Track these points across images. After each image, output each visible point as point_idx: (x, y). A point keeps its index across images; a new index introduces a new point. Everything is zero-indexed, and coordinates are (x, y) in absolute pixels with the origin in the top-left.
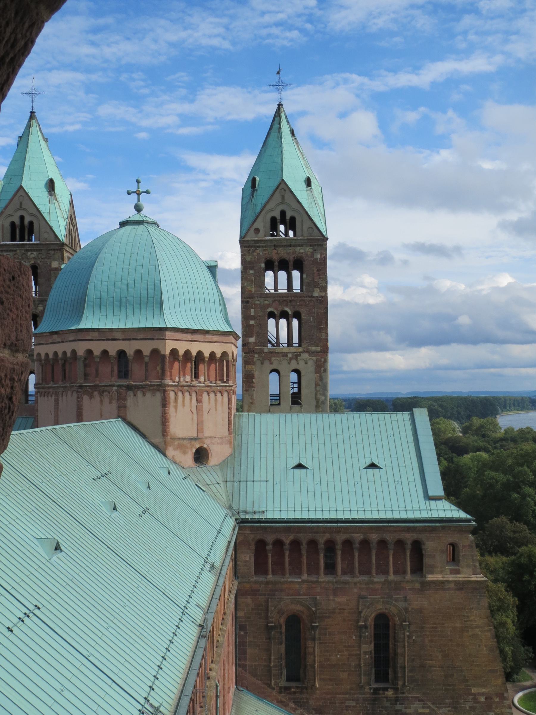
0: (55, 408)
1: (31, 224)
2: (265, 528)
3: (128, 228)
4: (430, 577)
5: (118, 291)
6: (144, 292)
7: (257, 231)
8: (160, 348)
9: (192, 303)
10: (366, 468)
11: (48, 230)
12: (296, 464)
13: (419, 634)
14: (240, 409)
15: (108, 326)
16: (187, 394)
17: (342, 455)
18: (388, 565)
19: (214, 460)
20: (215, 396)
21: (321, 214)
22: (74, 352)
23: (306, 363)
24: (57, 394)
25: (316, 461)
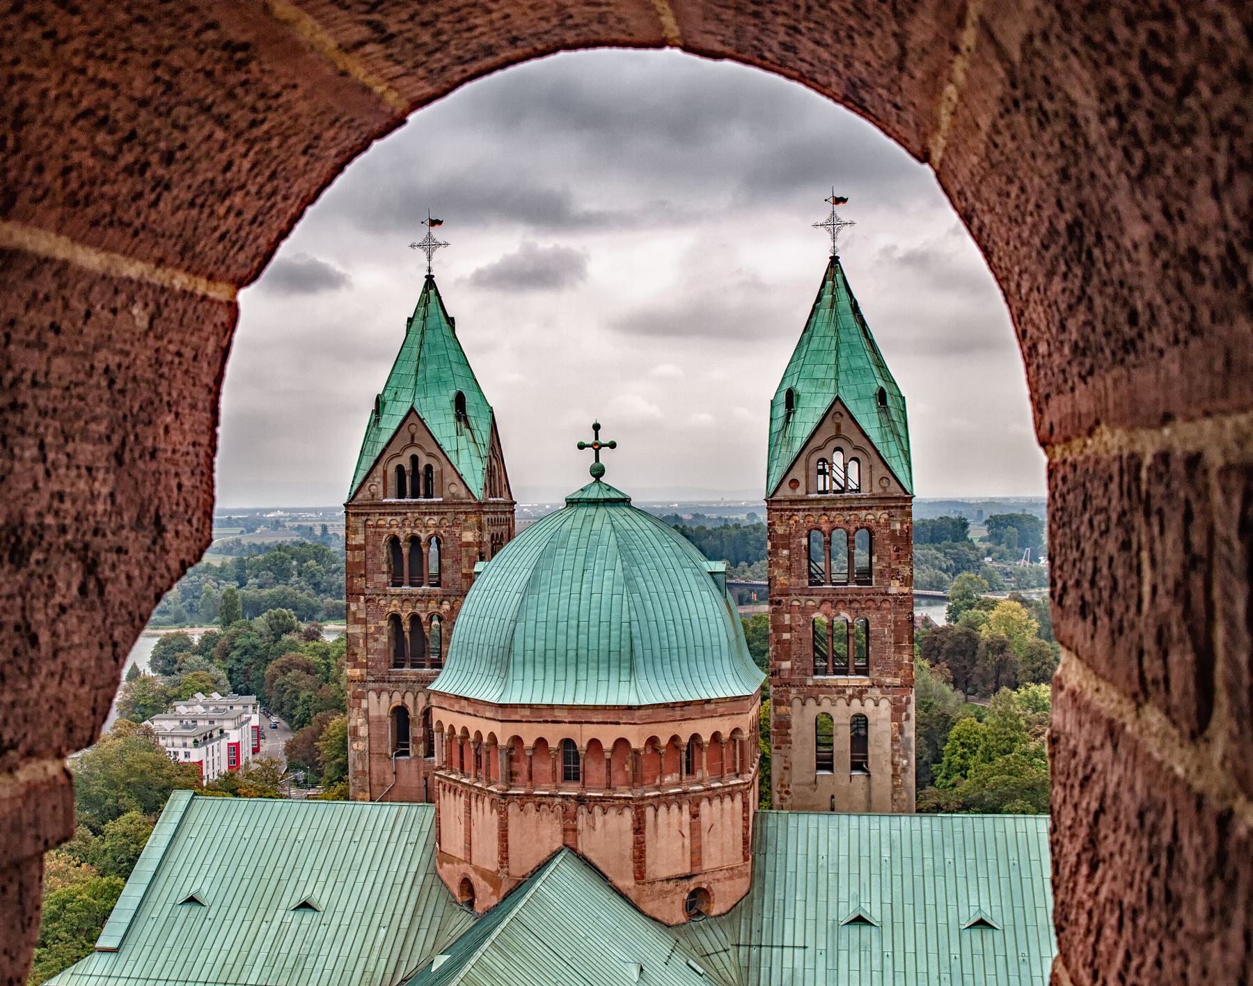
1: (429, 468)
3: (582, 512)
7: (794, 483)
11: (457, 481)
16: (674, 807)
23: (877, 705)
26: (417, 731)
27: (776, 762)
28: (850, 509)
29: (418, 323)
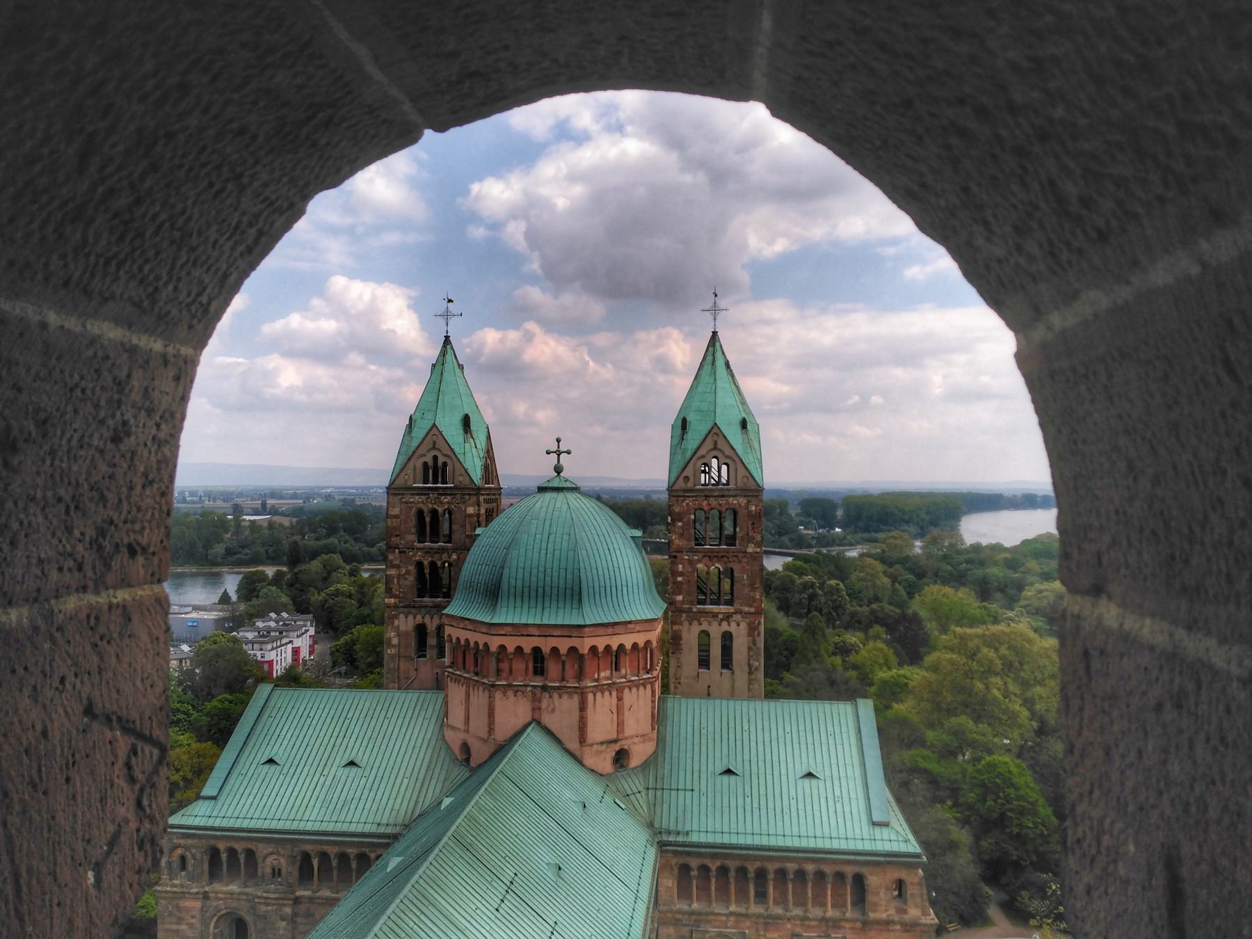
1: (445, 464)
2: (689, 854)
3: (548, 495)
4: (872, 915)
7: (687, 478)
9: (614, 589)
11: (464, 473)
15: (524, 621)
16: (607, 693)
18: (825, 897)
19: (635, 762)
22: (486, 644)
23: (738, 625)
24: (468, 687)
26: (432, 641)
27: (673, 663)
28: (723, 496)
29: (438, 368)
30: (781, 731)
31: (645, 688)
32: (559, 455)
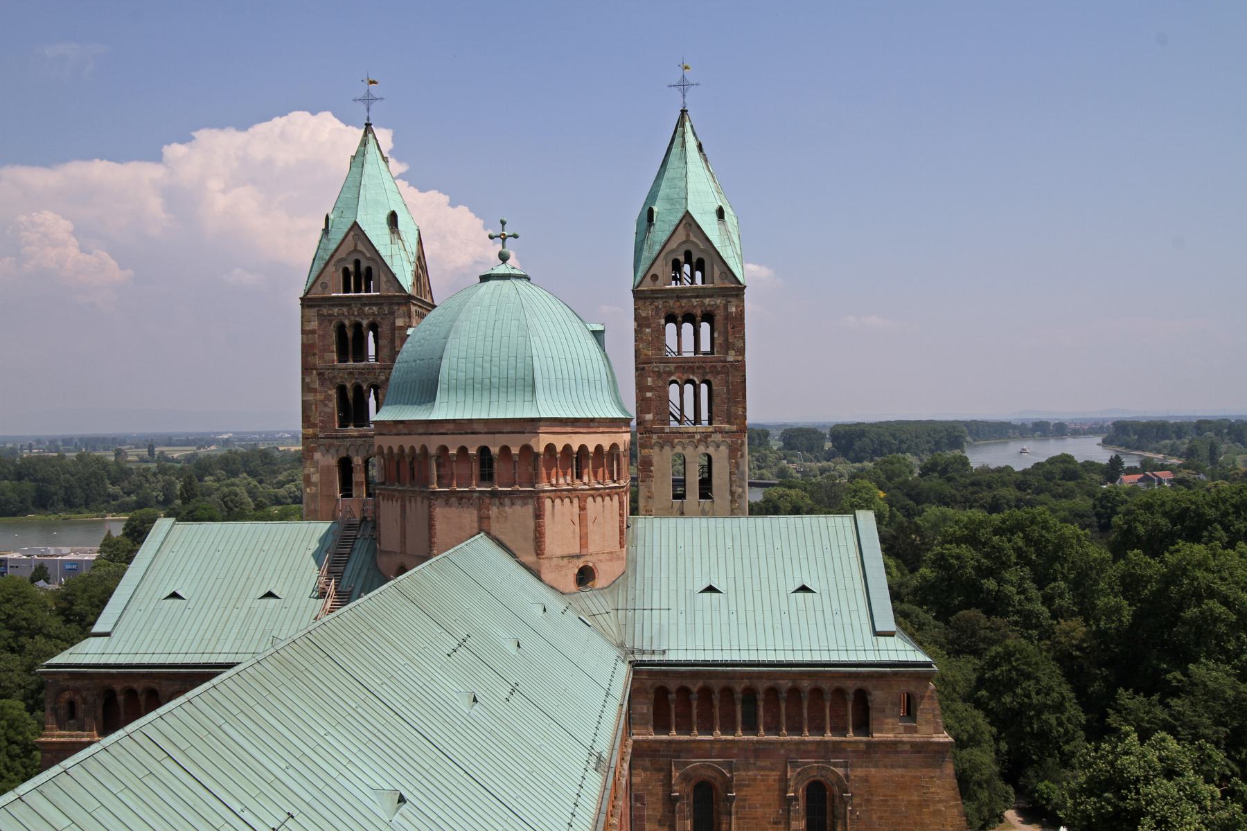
0: (401, 516)
1: (369, 270)
2: (666, 673)
3: (492, 283)
4: (877, 736)
5: (478, 369)
6: (512, 372)
7: (655, 277)
8: (532, 443)
9: (573, 382)
10: (795, 592)
12: (705, 586)
13: (864, 808)
14: (634, 511)
16: (567, 501)
17: (764, 575)
18: (824, 720)
19: (600, 582)
20: (603, 501)
21: (737, 254)
22: (424, 448)
25: (731, 581)
26: (358, 477)
27: (643, 492)
29: (359, 159)
30: (769, 547)
31: (611, 500)
32: (504, 240)
